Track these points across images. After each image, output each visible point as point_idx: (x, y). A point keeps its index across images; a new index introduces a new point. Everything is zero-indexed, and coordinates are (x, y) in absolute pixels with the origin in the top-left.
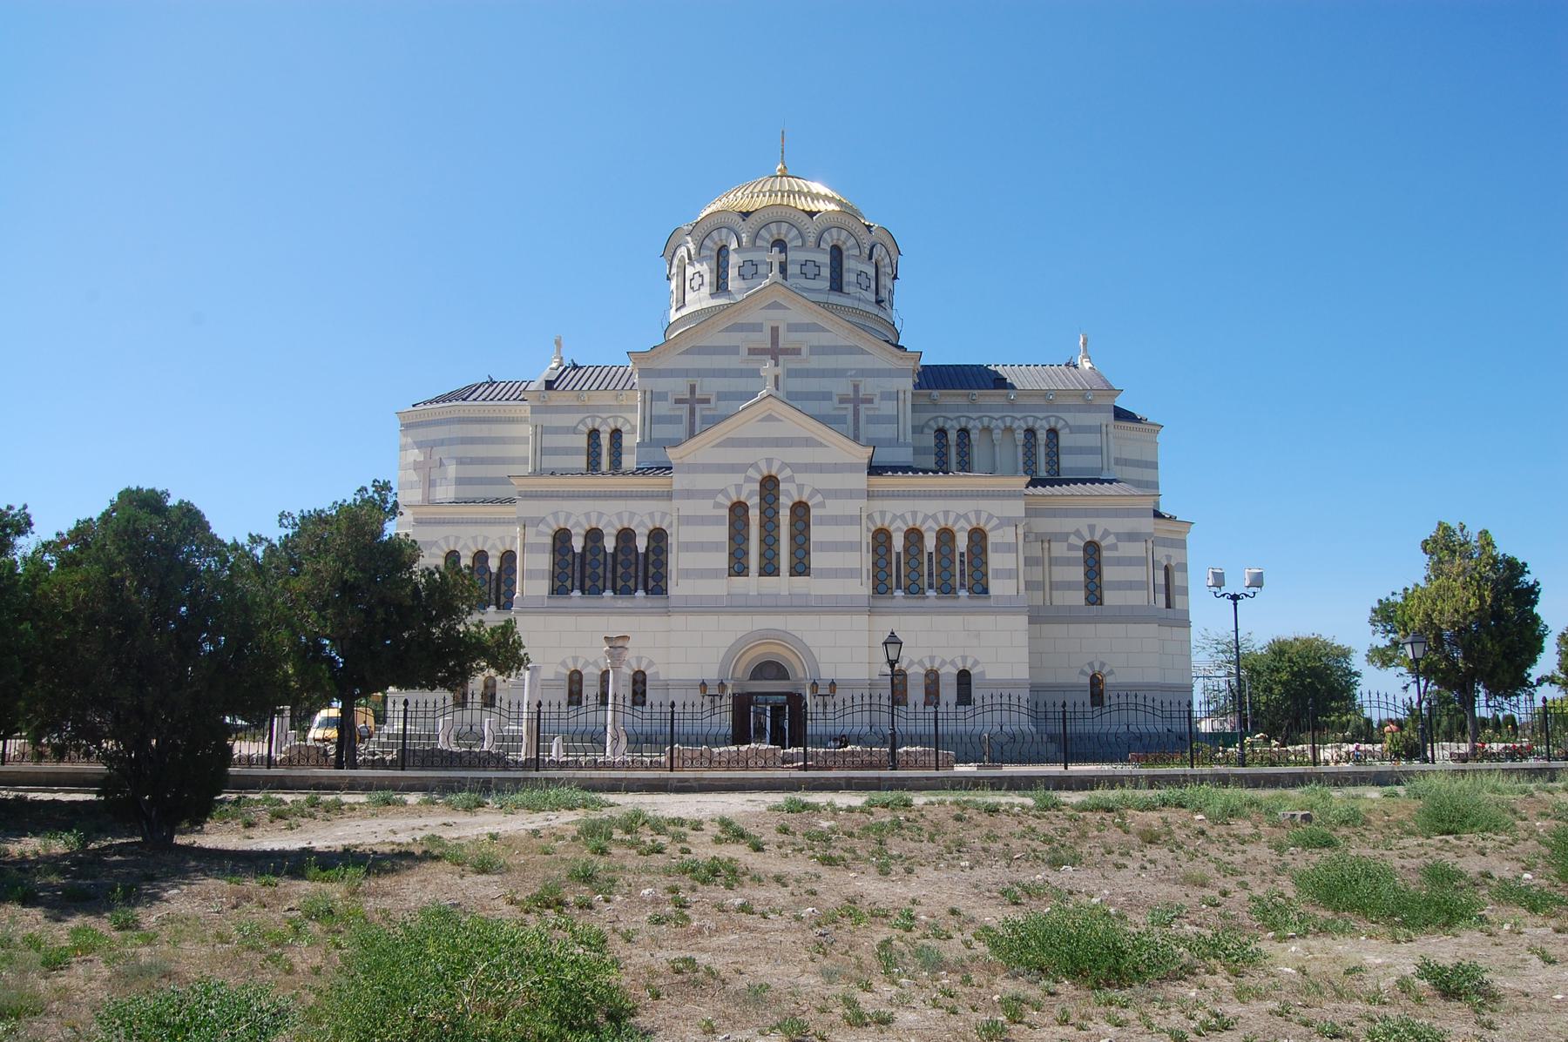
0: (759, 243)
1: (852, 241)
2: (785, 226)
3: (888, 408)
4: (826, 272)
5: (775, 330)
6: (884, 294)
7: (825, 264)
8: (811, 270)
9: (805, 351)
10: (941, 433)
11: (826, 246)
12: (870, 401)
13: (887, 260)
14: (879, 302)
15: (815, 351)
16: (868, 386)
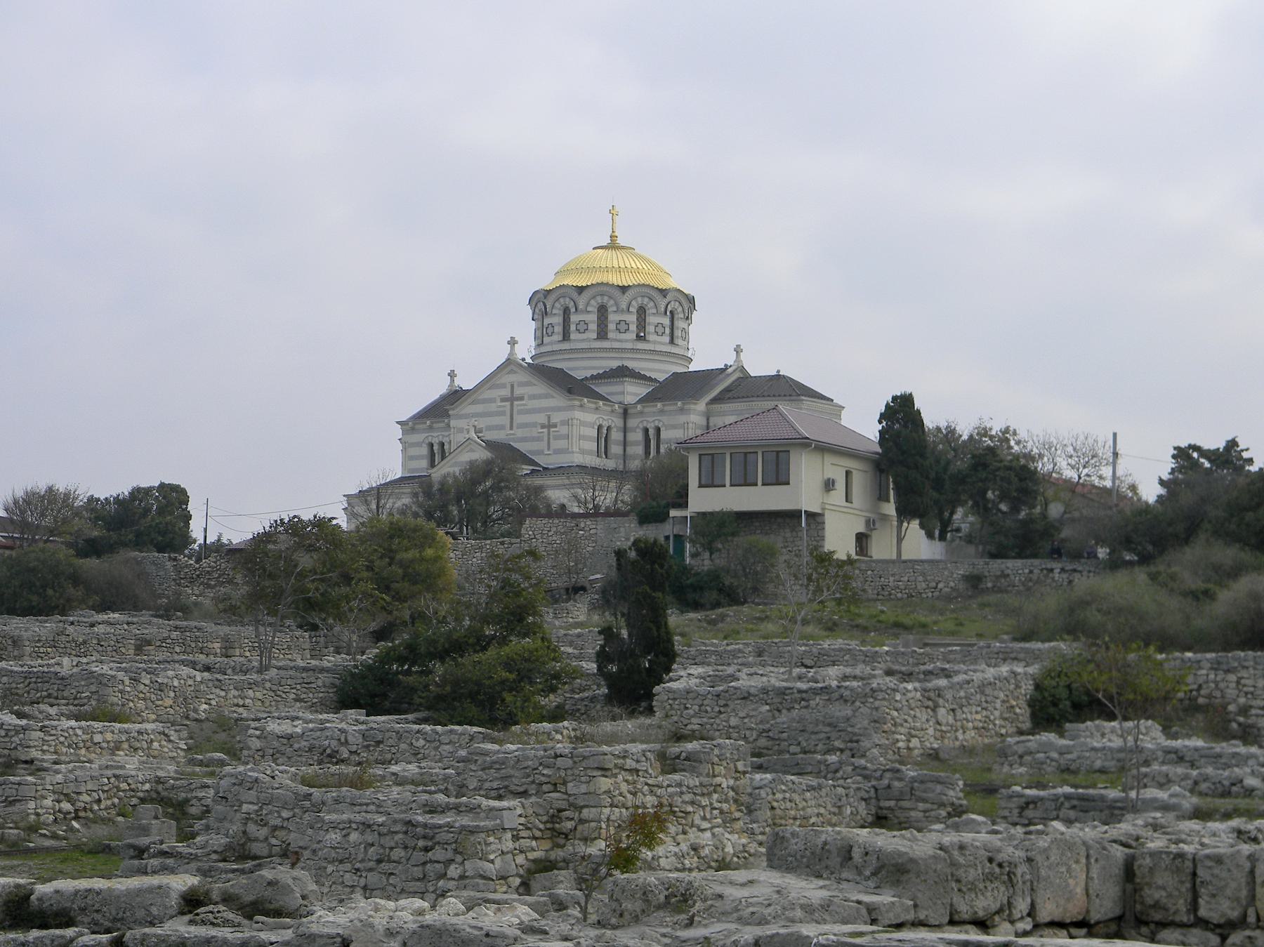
0: (554, 311)
1: (612, 302)
2: (568, 299)
3: (563, 430)
4: (593, 327)
5: (512, 386)
6: (650, 329)
7: (592, 322)
8: (582, 327)
9: (526, 397)
10: (646, 431)
11: (593, 308)
12: (556, 426)
13: (652, 304)
14: (639, 338)
15: (533, 397)
16: (556, 418)
